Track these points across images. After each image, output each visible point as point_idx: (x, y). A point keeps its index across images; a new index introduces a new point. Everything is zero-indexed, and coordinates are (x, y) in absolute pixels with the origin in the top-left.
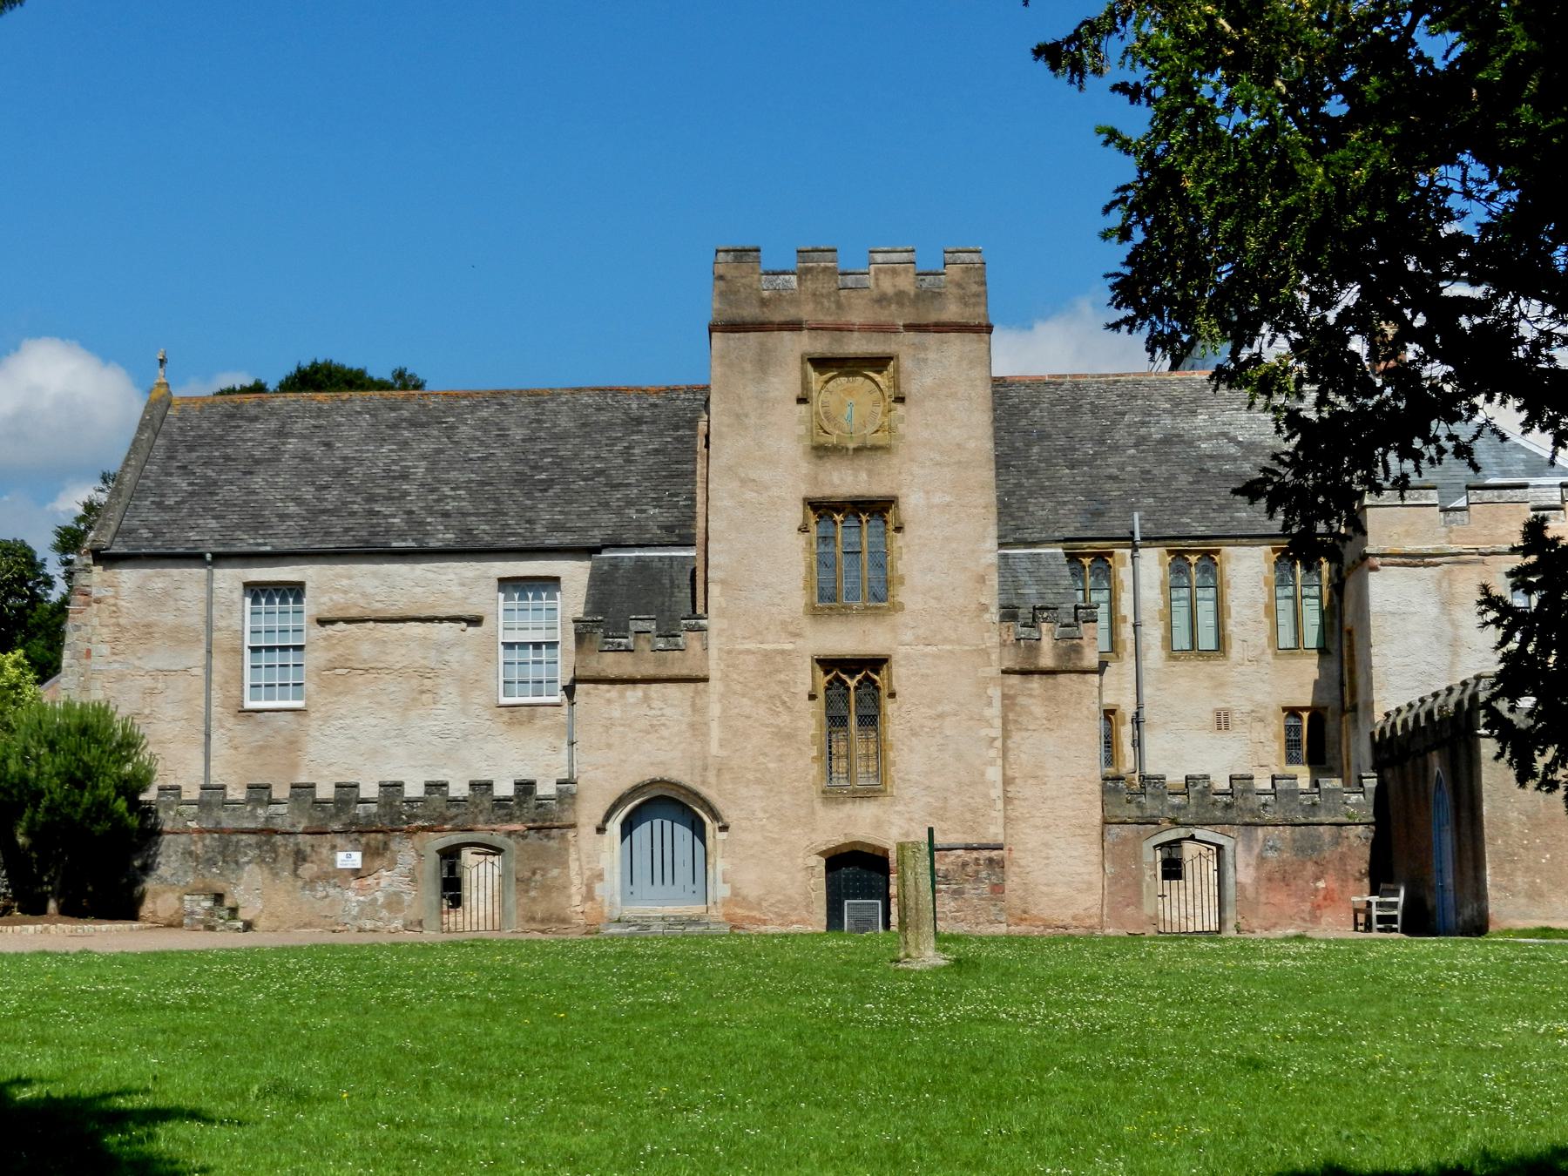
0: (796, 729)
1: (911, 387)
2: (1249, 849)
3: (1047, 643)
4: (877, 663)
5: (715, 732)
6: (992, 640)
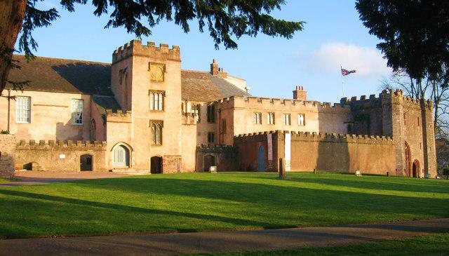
5: (133, 133)
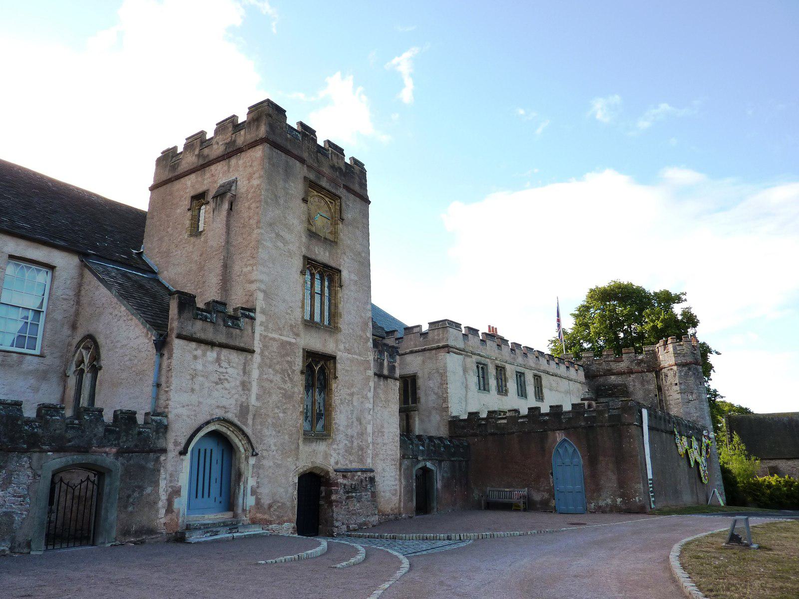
0: (294, 393)
2: (440, 472)
4: (333, 358)
5: (255, 389)
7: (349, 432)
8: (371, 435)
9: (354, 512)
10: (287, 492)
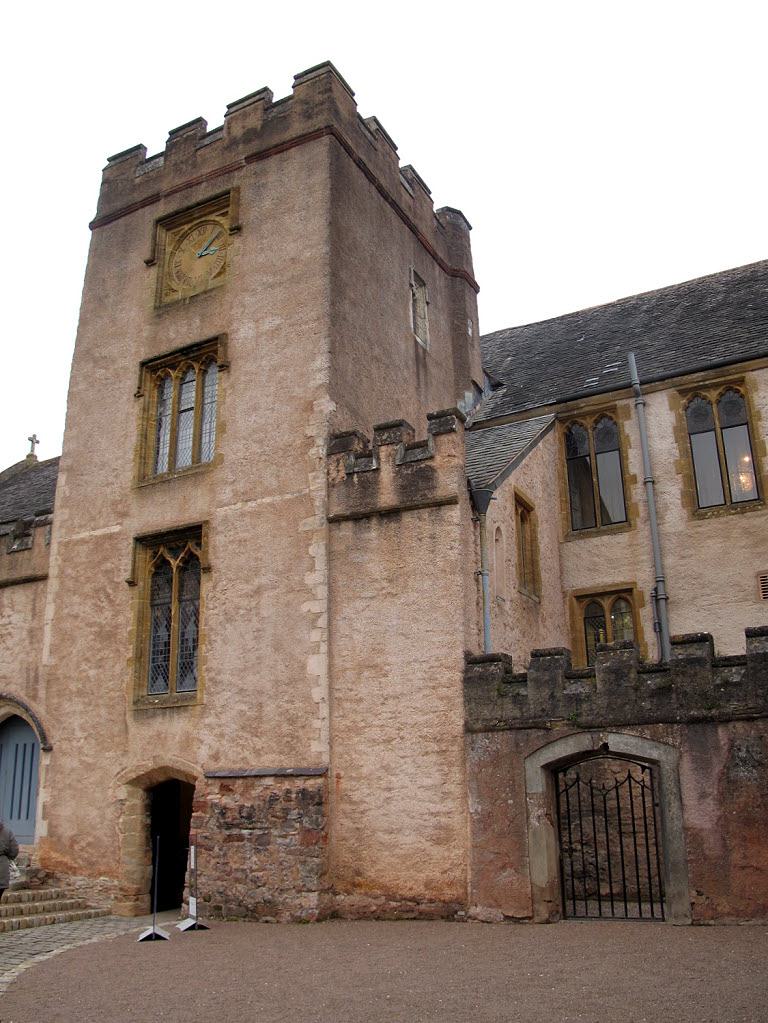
1: (249, 216)
2: (702, 766)
3: (387, 474)
4: (193, 533)
5: (48, 638)
6: (317, 484)
7: (251, 681)
8: (324, 681)
9: (239, 875)
10: (103, 817)
